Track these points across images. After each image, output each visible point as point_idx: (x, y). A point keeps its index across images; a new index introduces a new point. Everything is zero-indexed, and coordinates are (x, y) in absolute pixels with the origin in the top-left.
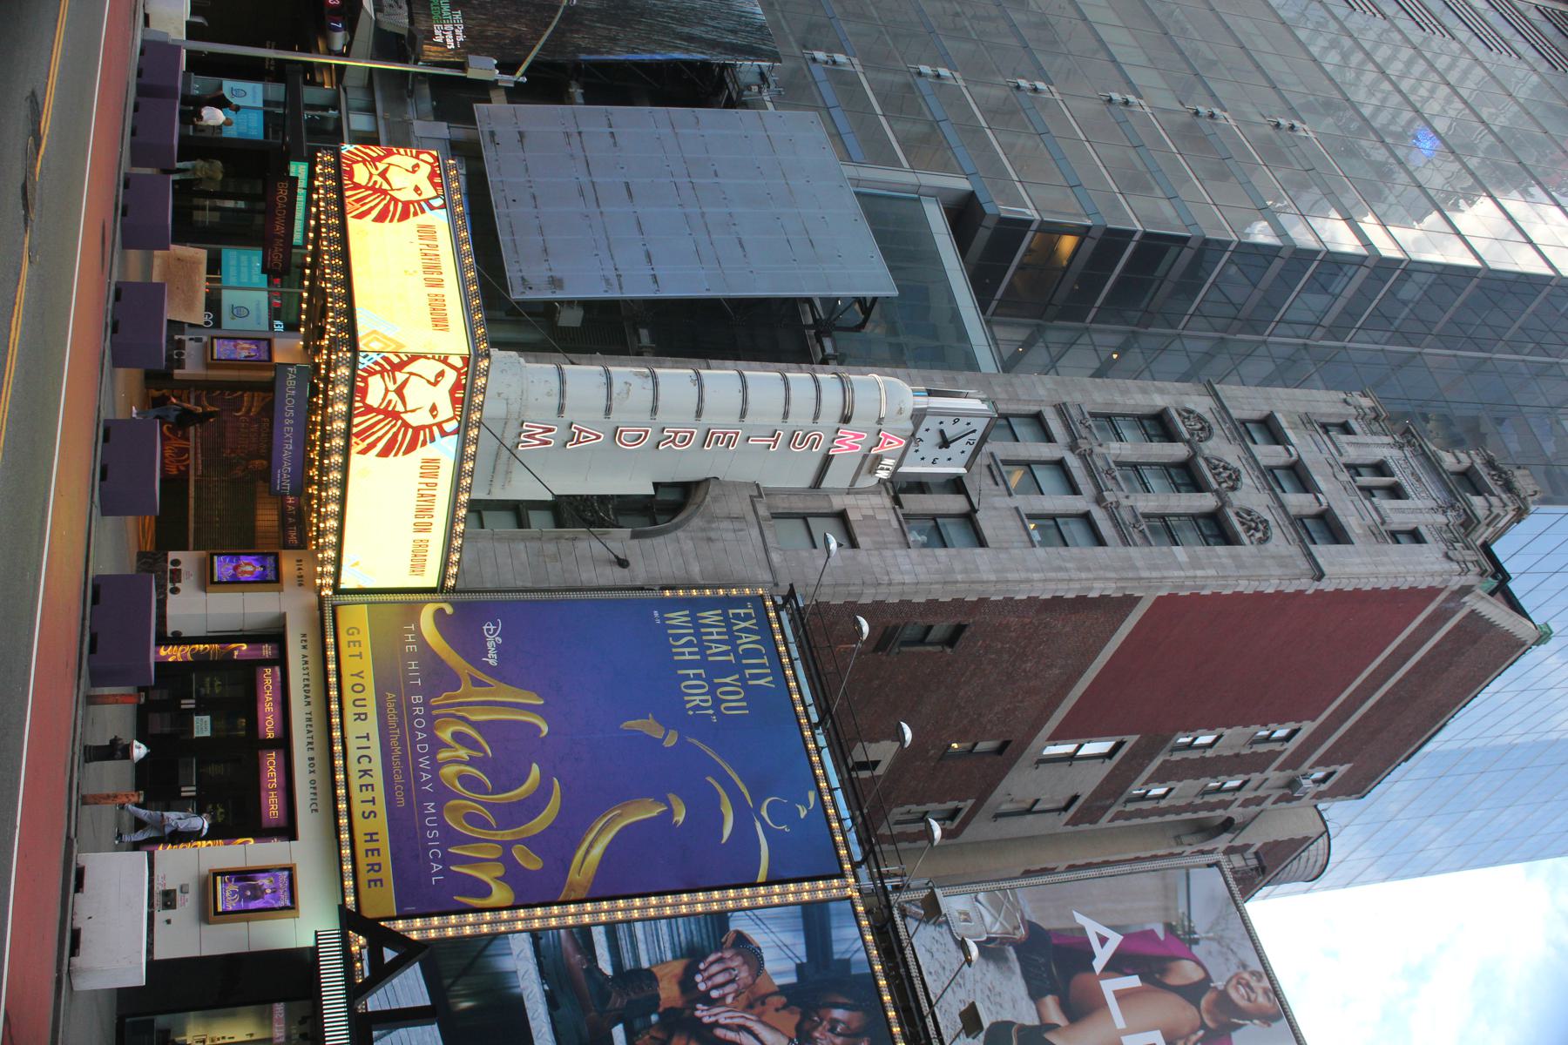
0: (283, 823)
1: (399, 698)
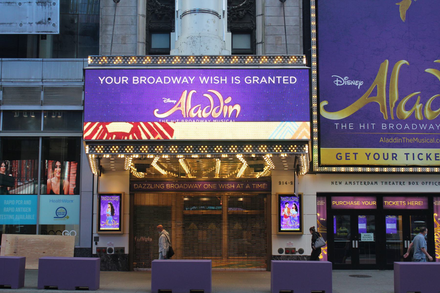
0: (426, 199)
1: (383, 136)
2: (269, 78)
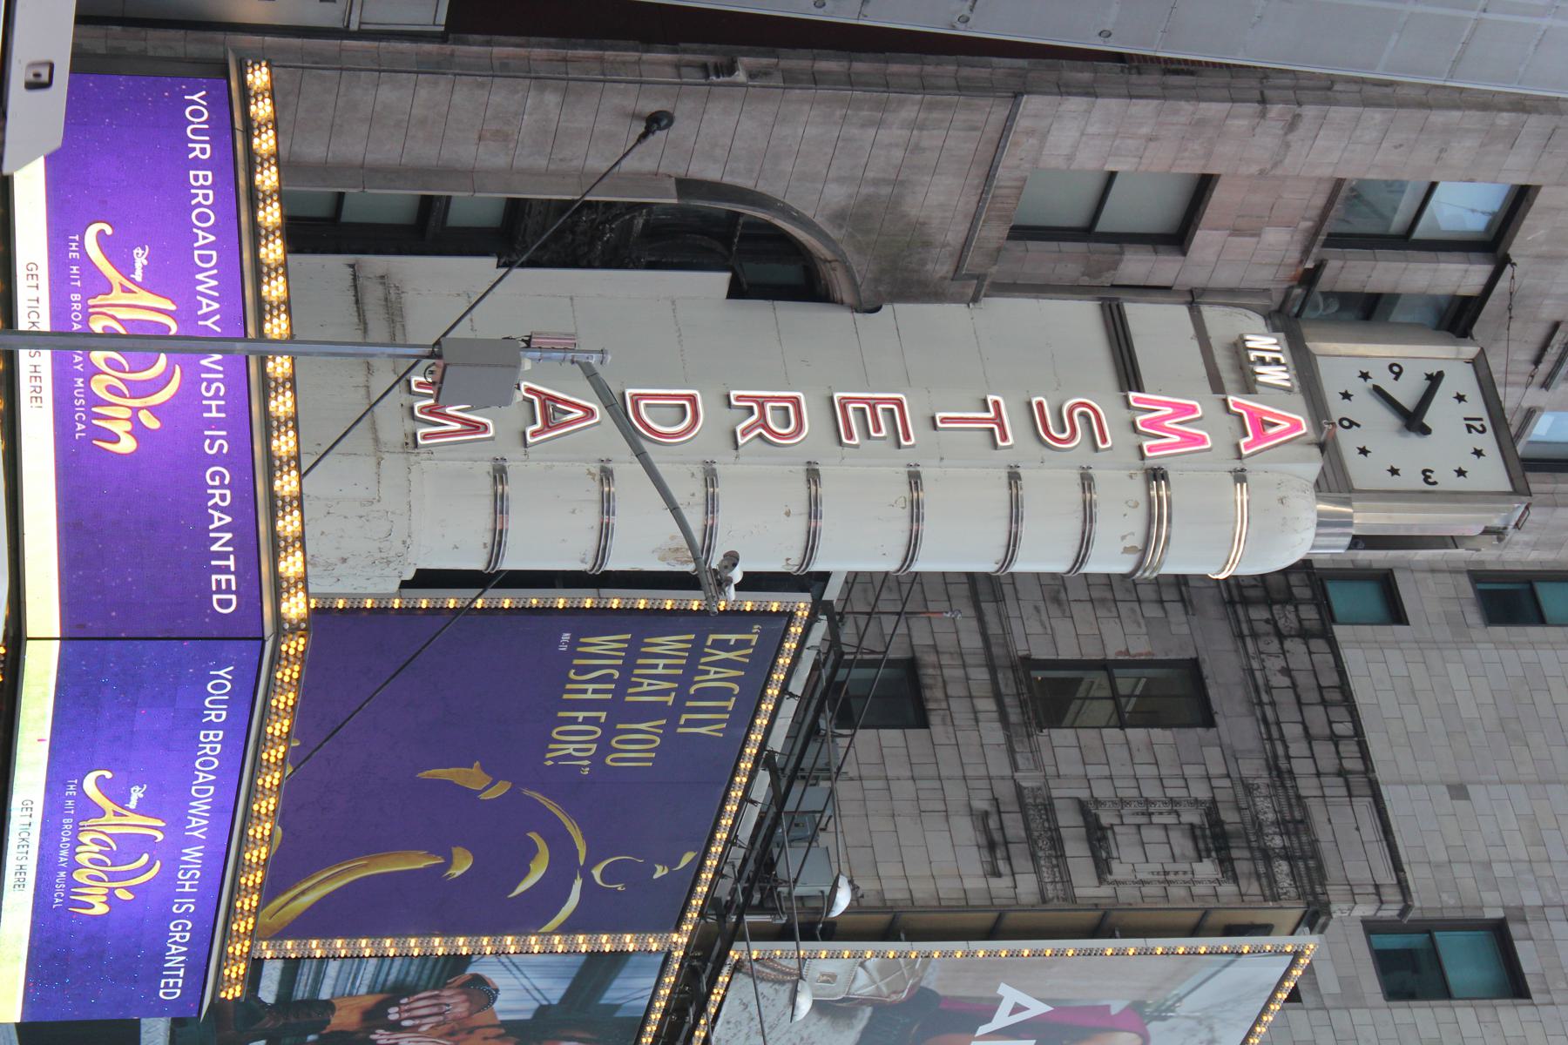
2: (228, 536)
